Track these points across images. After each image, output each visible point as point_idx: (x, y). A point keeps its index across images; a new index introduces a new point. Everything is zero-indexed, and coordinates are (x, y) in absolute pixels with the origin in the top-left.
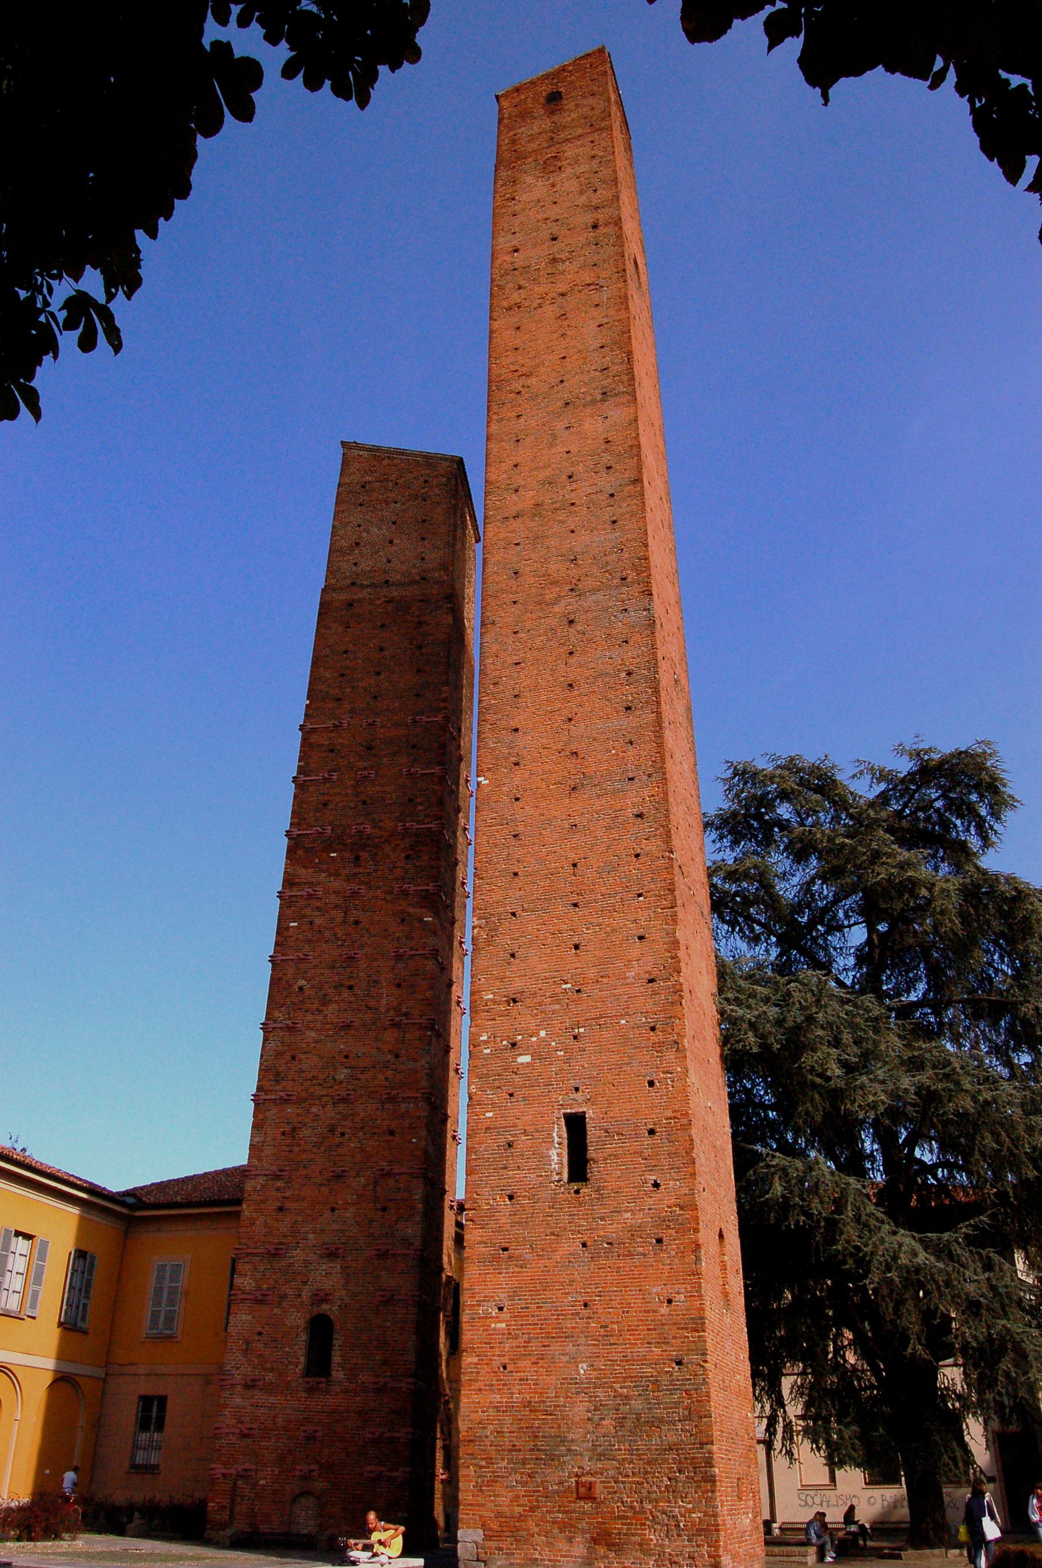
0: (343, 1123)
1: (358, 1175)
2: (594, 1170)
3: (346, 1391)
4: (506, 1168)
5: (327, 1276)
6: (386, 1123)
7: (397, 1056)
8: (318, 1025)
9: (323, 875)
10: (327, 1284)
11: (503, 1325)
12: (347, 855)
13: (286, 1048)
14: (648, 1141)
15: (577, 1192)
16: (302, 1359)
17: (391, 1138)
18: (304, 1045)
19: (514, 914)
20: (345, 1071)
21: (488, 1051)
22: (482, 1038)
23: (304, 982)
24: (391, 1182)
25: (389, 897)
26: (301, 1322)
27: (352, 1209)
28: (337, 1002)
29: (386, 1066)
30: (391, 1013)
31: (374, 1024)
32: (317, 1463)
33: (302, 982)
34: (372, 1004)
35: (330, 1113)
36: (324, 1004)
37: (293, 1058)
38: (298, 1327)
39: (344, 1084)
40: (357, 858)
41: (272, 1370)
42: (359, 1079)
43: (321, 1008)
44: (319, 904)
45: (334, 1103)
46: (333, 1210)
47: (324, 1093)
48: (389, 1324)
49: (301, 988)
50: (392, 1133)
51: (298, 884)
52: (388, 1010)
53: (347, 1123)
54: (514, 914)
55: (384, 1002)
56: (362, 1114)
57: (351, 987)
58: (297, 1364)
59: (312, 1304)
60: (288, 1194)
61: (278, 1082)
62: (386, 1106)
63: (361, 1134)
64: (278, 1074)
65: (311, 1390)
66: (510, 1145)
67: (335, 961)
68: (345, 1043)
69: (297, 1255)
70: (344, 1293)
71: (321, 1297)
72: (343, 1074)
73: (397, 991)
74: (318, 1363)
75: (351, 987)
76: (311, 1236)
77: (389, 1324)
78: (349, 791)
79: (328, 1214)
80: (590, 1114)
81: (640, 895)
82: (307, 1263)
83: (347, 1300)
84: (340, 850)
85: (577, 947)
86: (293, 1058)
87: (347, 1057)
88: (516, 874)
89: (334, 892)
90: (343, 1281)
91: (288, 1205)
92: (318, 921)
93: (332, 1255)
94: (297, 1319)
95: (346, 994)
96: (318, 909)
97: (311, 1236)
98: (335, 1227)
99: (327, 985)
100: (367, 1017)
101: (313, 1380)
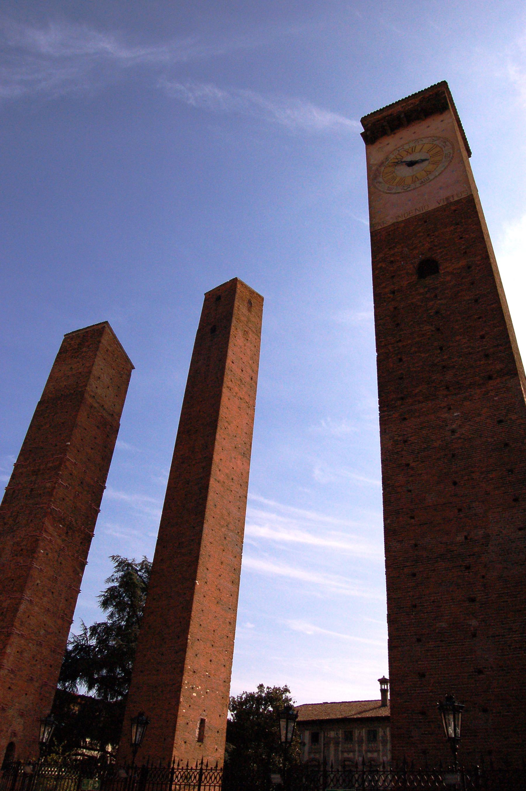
2: (205, 740)
9: (56, 534)
12: (65, 529)
14: (217, 734)
15: (200, 746)
25: (72, 558)
33: (39, 582)
36: (43, 596)
40: (67, 533)
44: (52, 547)
46: (26, 694)
51: (47, 532)
55: (61, 605)
57: (53, 593)
60: (14, 682)
64: (22, 622)
66: (187, 724)
70: (22, 734)
85: (211, 661)
91: (13, 687)
92: (50, 555)
96: (51, 549)
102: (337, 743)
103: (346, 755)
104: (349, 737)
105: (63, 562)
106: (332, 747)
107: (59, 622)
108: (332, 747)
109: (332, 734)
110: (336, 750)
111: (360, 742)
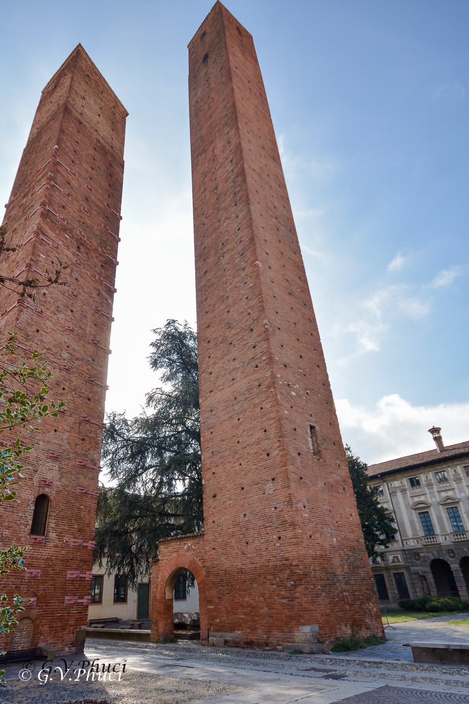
0: (64, 382)
1: (71, 416)
3: (56, 546)
4: (295, 440)
5: (50, 471)
6: (86, 393)
7: (93, 360)
8: (54, 321)
10: (49, 476)
11: (307, 515)
13: (34, 323)
16: (30, 522)
17: (89, 402)
18: (44, 327)
19: (279, 329)
20: (67, 354)
21: (281, 383)
22: (278, 376)
23: (46, 292)
24: (88, 426)
26: (32, 498)
27: (67, 434)
28: (65, 314)
29: (88, 363)
30: (92, 337)
31: (83, 337)
32: (36, 596)
34: (83, 327)
35: (56, 374)
37: (38, 331)
38: (29, 500)
39: (66, 361)
41: (9, 527)
42: (74, 363)
43: (56, 313)
44: (58, 256)
45: (60, 369)
46: (55, 431)
47: (55, 360)
48: (82, 507)
49: (44, 294)
50: (89, 400)
52: (90, 334)
53: (67, 384)
54: (279, 329)
56: (75, 383)
57: (72, 311)
58: (26, 526)
59: (40, 487)
61: (27, 340)
62: (87, 384)
63: (74, 393)
64: (28, 335)
65: (36, 544)
67: (65, 292)
68: (68, 339)
69: (33, 453)
71: (46, 483)
72: (66, 355)
73: (95, 327)
74: (38, 527)
75: (72, 311)
76: (41, 443)
77: (82, 507)
78: (76, 211)
79: (53, 432)
80: (317, 428)
81: (315, 350)
82: (38, 459)
83: (61, 488)
84: (70, 236)
86: (38, 331)
87: (68, 347)
88: (277, 313)
89: (66, 256)
90: (59, 476)
93: (55, 458)
94: (28, 496)
95: (69, 313)
97: (41, 443)
98: (56, 441)
99: (59, 302)
100: (80, 331)
101: (39, 538)
102: (404, 491)
103: (416, 499)
104: (415, 483)
105: (80, 279)
106: (399, 495)
107: (90, 348)
108: (399, 495)
109: (396, 484)
110: (405, 498)
111: (430, 485)
